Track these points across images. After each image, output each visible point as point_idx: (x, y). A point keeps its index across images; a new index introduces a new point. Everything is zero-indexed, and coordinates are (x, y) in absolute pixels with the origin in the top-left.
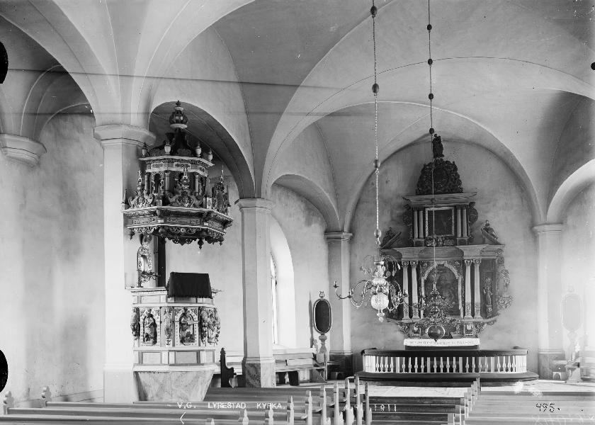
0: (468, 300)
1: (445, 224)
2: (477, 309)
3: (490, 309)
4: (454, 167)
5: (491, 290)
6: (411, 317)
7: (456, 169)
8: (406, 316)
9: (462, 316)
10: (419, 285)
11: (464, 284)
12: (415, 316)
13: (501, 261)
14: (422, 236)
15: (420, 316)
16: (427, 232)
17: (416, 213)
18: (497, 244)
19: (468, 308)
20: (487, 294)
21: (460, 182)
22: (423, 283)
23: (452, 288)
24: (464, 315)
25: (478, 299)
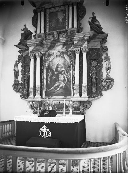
0: (77, 82)
1: (61, 20)
2: (84, 88)
3: (94, 89)
5: (97, 74)
6: (34, 96)
8: (31, 96)
9: (72, 94)
11: (74, 70)
12: (38, 96)
13: (105, 49)
14: (43, 31)
16: (47, 31)
17: (39, 14)
18: (103, 33)
20: (92, 78)
22: (45, 71)
23: (66, 74)
24: (74, 95)
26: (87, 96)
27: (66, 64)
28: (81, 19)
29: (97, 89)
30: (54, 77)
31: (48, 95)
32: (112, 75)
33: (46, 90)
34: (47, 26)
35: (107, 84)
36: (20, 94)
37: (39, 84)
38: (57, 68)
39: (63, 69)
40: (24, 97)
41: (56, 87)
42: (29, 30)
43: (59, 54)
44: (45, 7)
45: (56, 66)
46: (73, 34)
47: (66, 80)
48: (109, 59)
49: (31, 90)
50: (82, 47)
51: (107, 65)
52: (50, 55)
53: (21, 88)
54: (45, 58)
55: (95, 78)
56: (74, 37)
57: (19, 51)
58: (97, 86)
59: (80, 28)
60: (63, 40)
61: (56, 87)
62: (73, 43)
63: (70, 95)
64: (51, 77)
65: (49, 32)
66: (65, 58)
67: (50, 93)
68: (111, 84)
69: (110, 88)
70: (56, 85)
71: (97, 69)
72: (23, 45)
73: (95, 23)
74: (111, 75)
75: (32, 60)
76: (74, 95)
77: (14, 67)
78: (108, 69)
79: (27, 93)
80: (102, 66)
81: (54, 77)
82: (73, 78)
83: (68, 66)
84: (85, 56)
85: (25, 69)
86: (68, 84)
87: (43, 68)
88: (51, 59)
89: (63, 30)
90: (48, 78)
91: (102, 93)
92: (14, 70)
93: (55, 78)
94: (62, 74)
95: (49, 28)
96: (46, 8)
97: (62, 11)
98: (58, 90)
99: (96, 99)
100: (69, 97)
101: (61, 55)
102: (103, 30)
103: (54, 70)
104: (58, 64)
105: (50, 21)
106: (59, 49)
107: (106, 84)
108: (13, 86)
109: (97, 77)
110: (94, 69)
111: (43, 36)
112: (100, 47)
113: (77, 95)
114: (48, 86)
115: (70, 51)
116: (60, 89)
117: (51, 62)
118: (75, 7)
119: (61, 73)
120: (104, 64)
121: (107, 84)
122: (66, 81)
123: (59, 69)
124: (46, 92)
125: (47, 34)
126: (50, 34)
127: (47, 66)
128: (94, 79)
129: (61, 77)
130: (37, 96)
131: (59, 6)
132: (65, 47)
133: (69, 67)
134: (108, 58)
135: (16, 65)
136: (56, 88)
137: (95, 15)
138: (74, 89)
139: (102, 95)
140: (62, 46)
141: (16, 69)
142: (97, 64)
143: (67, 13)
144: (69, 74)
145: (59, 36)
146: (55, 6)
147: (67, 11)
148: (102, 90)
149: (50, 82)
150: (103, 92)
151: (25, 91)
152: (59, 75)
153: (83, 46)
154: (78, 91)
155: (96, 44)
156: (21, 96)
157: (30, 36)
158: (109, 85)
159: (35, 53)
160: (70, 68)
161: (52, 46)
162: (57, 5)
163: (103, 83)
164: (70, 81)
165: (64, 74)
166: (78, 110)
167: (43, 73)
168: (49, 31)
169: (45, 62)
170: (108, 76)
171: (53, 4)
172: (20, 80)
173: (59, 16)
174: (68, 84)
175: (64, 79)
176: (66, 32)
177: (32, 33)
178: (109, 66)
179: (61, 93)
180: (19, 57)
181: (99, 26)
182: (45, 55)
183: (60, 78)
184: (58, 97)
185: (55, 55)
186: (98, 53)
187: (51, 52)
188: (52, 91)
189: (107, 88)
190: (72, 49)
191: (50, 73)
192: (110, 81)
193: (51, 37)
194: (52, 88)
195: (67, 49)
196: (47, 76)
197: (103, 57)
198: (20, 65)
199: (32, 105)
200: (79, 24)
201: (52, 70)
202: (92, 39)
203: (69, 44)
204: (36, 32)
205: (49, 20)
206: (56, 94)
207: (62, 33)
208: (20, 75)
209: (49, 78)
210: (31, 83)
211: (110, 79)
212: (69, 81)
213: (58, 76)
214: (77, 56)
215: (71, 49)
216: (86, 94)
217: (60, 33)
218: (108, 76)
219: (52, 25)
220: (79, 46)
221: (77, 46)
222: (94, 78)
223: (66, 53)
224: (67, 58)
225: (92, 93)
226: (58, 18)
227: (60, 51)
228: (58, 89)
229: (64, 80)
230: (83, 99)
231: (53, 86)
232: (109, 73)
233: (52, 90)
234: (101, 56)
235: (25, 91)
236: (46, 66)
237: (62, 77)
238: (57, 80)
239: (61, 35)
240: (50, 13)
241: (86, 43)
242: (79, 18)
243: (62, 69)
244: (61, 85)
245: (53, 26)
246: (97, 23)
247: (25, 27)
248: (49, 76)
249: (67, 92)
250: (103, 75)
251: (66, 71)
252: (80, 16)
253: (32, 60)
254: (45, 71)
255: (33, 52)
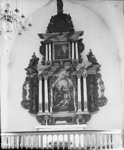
0: (79, 99)
1: (65, 51)
2: (85, 105)
3: (93, 106)
4: (69, 17)
5: (94, 93)
6: (44, 111)
7: (70, 18)
8: (41, 111)
9: (76, 110)
10: (49, 91)
11: (77, 90)
12: (47, 111)
13: (99, 76)
14: (50, 59)
15: (49, 111)
16: (54, 58)
17: (47, 46)
18: (98, 64)
19: (80, 104)
21: (72, 26)
22: (52, 90)
23: (70, 93)
24: (77, 110)
25: (86, 99)
26: (88, 111)
27: (69, 85)
28: (81, 53)
29: (94, 105)
31: (55, 110)
32: (106, 95)
33: (53, 106)
34: (54, 55)
35: (102, 101)
36: (28, 110)
37: (47, 102)
38: (62, 88)
39: (67, 90)
40: (32, 113)
41: (62, 104)
42: (37, 57)
43: (63, 77)
44: (52, 41)
45: (61, 87)
46: (76, 63)
47: (70, 98)
48: (103, 83)
49: (41, 107)
50: (83, 73)
51: (101, 87)
52: (56, 78)
53: (29, 105)
54: (51, 81)
55: (93, 97)
56: (77, 66)
57: (27, 73)
58: (94, 103)
59: (81, 59)
60: (67, 67)
61: (62, 104)
62: (75, 70)
63: (74, 110)
64: (57, 96)
65: (55, 60)
66: (68, 81)
67: (57, 109)
68: (105, 102)
69: (104, 104)
70: (62, 102)
71: (94, 90)
72: (32, 68)
73: (92, 56)
74: (104, 95)
75: (40, 82)
76: (77, 110)
77: (23, 87)
78: (103, 91)
79: (35, 109)
80: (98, 88)
82: (76, 96)
83: (71, 87)
84: (85, 80)
85: (32, 89)
86: (71, 102)
87: (50, 88)
88: (56, 81)
89: (68, 59)
90: (54, 97)
91: (99, 108)
92: (23, 89)
93: (61, 96)
94: (66, 94)
95: (55, 57)
96: (52, 41)
97: (65, 44)
98: (63, 107)
99: (95, 113)
100: (73, 112)
101: (65, 78)
102: (97, 62)
103: (60, 90)
104: (62, 86)
105: (55, 52)
106: (63, 73)
107: (101, 101)
108: (21, 104)
109: (94, 96)
110: (91, 90)
111: (51, 63)
112: (95, 74)
113: (80, 110)
114: (55, 103)
115: (73, 75)
116: (65, 105)
118: (76, 44)
119: (65, 92)
120: (99, 86)
121: (102, 101)
122: (70, 99)
123: (64, 89)
124: (53, 108)
125: (53, 62)
126: (56, 62)
127: (53, 86)
128: (92, 98)
129: (66, 96)
130: (46, 111)
131: (63, 41)
132: (68, 72)
133: (72, 88)
134: (102, 83)
135: (25, 85)
136: (61, 105)
137: (91, 51)
138: (77, 106)
139: (98, 110)
140: (66, 71)
141: (25, 88)
142: (94, 86)
143: (70, 47)
144: (72, 93)
145: (64, 64)
146: (61, 41)
147: (70, 45)
148: (98, 106)
149: (56, 100)
150: (99, 108)
151: (34, 108)
152: (64, 94)
153: (84, 73)
154: (81, 107)
155: (93, 72)
156: (29, 112)
157: (37, 62)
158: (104, 102)
159: (44, 76)
160: (73, 89)
161: (58, 71)
162: (62, 40)
163: (99, 101)
164: (73, 99)
165: (68, 93)
166: (81, 122)
167: (50, 92)
168: (55, 59)
169: (52, 84)
170: (102, 95)
171: (58, 39)
172: (27, 98)
173: (63, 48)
174: (71, 102)
175: (68, 97)
176: (70, 61)
177: (38, 59)
178: (103, 89)
179: (66, 108)
180: (27, 79)
181: (95, 59)
182: (51, 78)
183: (64, 97)
184: (64, 112)
185: (60, 78)
186: (94, 78)
187: (56, 75)
188: (58, 107)
189: (102, 105)
190: (74, 74)
191: (55, 92)
192: (104, 100)
193: (58, 64)
194: (58, 105)
195: (70, 74)
196: (54, 94)
197: (98, 81)
198: (28, 85)
199: (41, 119)
200: (80, 56)
201: (57, 90)
202: (90, 68)
203: (72, 70)
204: (44, 59)
205: (55, 50)
206: (62, 110)
207: (66, 62)
208: (28, 94)
209: (55, 97)
210: (40, 101)
211: (104, 98)
212: (72, 99)
213: (62, 95)
214: (79, 80)
215: (74, 73)
216: (87, 109)
217: (65, 61)
218: (102, 95)
219: (57, 55)
220: (80, 72)
221: (79, 72)
222: (92, 97)
223: (70, 77)
224: (70, 81)
225: (91, 108)
226: (62, 50)
227: (64, 75)
228: (64, 105)
229: (68, 98)
230: (85, 113)
231: (59, 103)
232: (103, 93)
233: (58, 106)
234: (96, 80)
235: (34, 108)
236: (52, 87)
237: (67, 96)
238: (62, 98)
239: (66, 63)
240: (55, 46)
241: (85, 70)
242: (80, 51)
243: (66, 90)
244: (66, 103)
245: (58, 55)
246: (93, 57)
247: (34, 54)
248: (55, 95)
249: (70, 108)
250: (98, 95)
251: (70, 91)
252: (80, 50)
253: (40, 82)
254: (52, 90)
255: (41, 75)
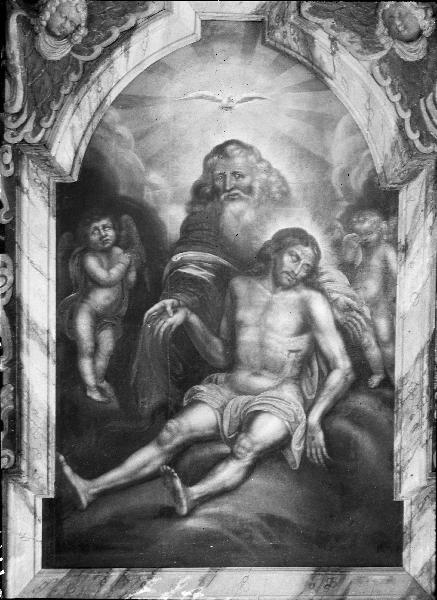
23: (333, 276)
27: (339, 150)
30: (169, 315)
33: (61, 481)
38: (208, 195)
41: (206, 452)
45: (192, 172)
47: (329, 366)
54: (31, 50)
61: (206, 452)
64: (129, 317)
66: (318, 78)
67: (117, 523)
70: (200, 418)
81: (169, 315)
83: (358, 182)
86: (357, 418)
88: (122, 70)
90: (83, 324)
93: (184, 330)
94: (278, 284)
98: (224, 492)
103: (174, 217)
104: (221, 150)
116: (250, 470)
117: (125, 101)
119: (261, 263)
122: (336, 379)
124: (57, 511)
127: (65, 152)
149: (117, 372)
152: (240, 286)
164: (387, 382)
165: (311, 279)
175: (302, 343)
179: (271, 519)
194: (147, 458)
196: (71, 288)
201: (140, 218)
206: (203, 539)
228: (228, 473)
229: (312, 362)
233: (135, 483)
236: (47, 163)
243: (280, 224)
244: (267, 429)
248: (101, 298)
251: (337, 245)
